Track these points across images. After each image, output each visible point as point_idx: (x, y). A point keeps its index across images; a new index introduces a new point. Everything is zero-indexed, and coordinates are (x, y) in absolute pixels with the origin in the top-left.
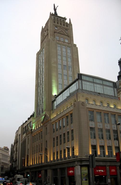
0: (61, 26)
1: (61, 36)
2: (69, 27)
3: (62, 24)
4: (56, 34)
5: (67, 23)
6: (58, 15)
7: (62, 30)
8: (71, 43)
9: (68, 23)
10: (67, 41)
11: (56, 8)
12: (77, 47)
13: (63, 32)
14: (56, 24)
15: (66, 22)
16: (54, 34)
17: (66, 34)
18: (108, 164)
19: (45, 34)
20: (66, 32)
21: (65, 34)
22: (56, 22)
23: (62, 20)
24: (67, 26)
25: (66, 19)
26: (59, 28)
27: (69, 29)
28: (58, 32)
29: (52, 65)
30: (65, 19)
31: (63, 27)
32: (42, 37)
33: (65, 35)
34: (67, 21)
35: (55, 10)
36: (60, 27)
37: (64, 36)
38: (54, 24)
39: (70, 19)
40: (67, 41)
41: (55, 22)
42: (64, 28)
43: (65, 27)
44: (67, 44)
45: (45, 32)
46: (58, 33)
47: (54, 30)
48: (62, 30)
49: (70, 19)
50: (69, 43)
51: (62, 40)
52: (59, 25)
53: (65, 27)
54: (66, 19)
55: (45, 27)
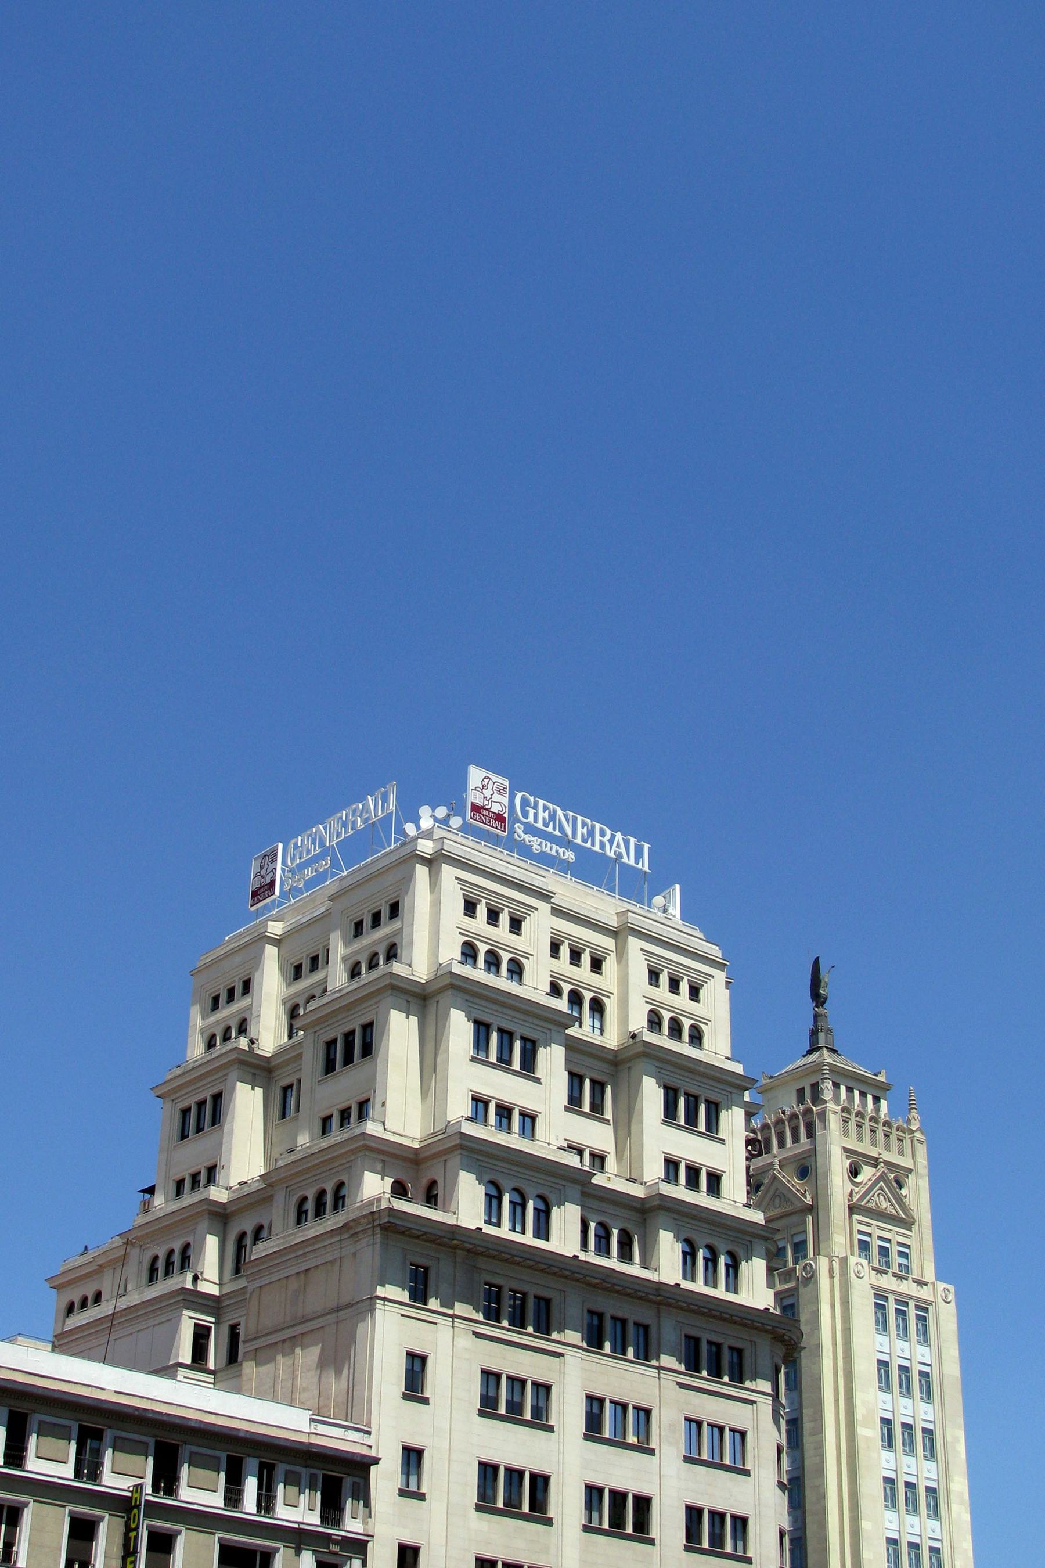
27: (910, 1171)
31: (886, 1163)
38: (846, 1150)
41: (846, 1133)
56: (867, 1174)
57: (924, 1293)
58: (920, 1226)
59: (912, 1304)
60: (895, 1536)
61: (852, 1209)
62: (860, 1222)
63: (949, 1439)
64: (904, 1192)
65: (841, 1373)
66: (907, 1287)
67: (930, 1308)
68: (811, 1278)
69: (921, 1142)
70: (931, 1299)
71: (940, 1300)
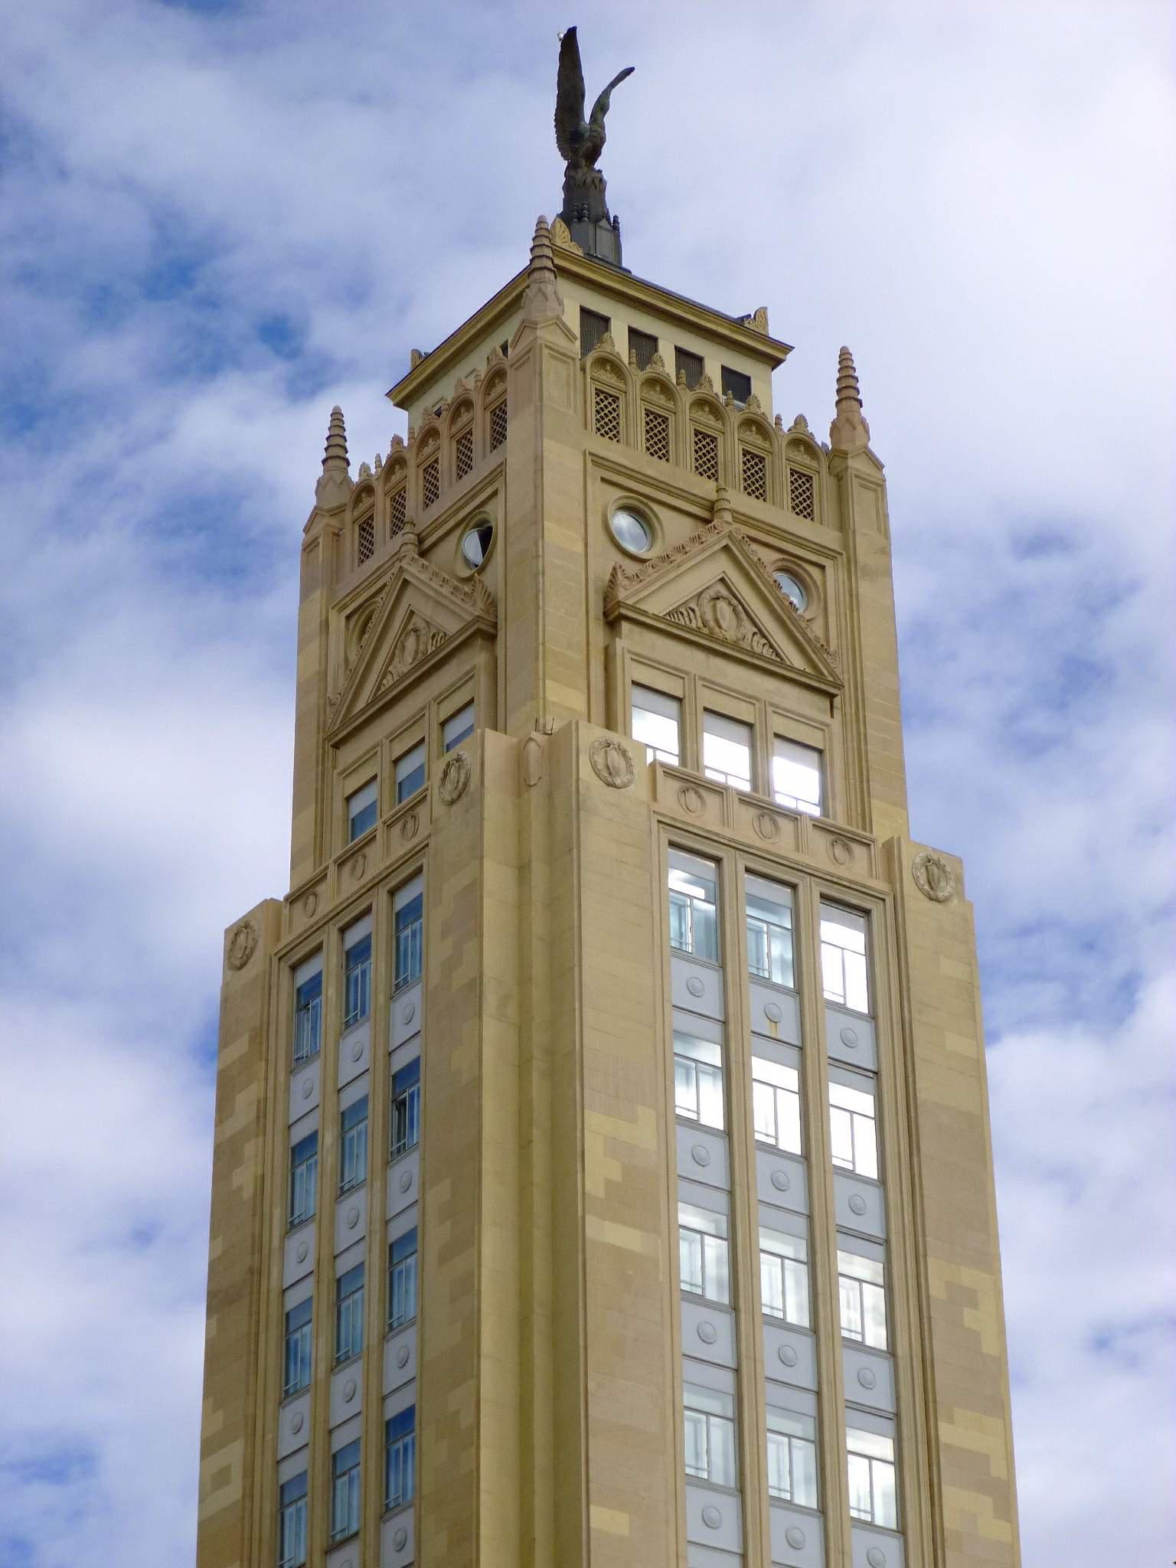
0: (706, 488)
1: (710, 684)
2: (843, 524)
3: (731, 450)
4: (629, 638)
5: (802, 442)
6: (640, 258)
8: (866, 822)
9: (822, 435)
10: (796, 783)
11: (602, 106)
13: (741, 610)
15: (787, 424)
16: (598, 634)
19: (410, 598)
20: (785, 617)
21: (781, 661)
23: (715, 361)
25: (773, 355)
26: (675, 527)
28: (657, 606)
29: (603, 1232)
30: (756, 345)
31: (741, 518)
32: (337, 621)
33: (773, 669)
34: (797, 396)
35: (579, 139)
36: (708, 514)
37: (771, 684)
38: (598, 461)
39: (845, 357)
40: (796, 783)
41: (608, 426)
42: (765, 534)
43: (777, 513)
44: (818, 853)
45: (413, 569)
46: (669, 629)
47: (604, 562)
48: (722, 566)
49: (845, 357)
50: (841, 822)
51: (725, 758)
52: (680, 471)
54: (773, 355)
55: (396, 462)
58: (860, 704)
62: (640, 659)
63: (936, 1289)
68: (464, 793)
70: (880, 885)
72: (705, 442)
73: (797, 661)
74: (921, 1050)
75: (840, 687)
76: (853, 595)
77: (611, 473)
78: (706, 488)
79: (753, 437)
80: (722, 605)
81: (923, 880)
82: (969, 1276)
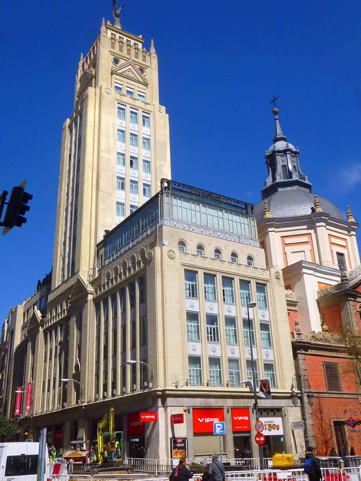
7: (132, 68)
12: (167, 115)
14: (117, 50)
17: (142, 81)
18: (230, 403)
22: (117, 45)
24: (144, 60)
27: (148, 67)
31: (133, 61)
36: (126, 59)
38: (110, 52)
41: (113, 47)
43: (140, 60)
46: (120, 75)
53: (140, 60)
56: (122, 62)
57: (149, 107)
58: (152, 87)
59: (140, 110)
60: (123, 201)
61: (112, 74)
62: (116, 79)
63: (158, 164)
64: (144, 74)
65: (96, 133)
66: (137, 103)
67: (151, 114)
69: (154, 57)
70: (152, 110)
71: (156, 110)
72: (129, 51)
73: (142, 81)
74: (157, 132)
75: (148, 84)
76: (152, 73)
77: (112, 53)
78: (128, 57)
79: (136, 50)
80: (130, 72)
81: (158, 109)
82: (163, 163)
